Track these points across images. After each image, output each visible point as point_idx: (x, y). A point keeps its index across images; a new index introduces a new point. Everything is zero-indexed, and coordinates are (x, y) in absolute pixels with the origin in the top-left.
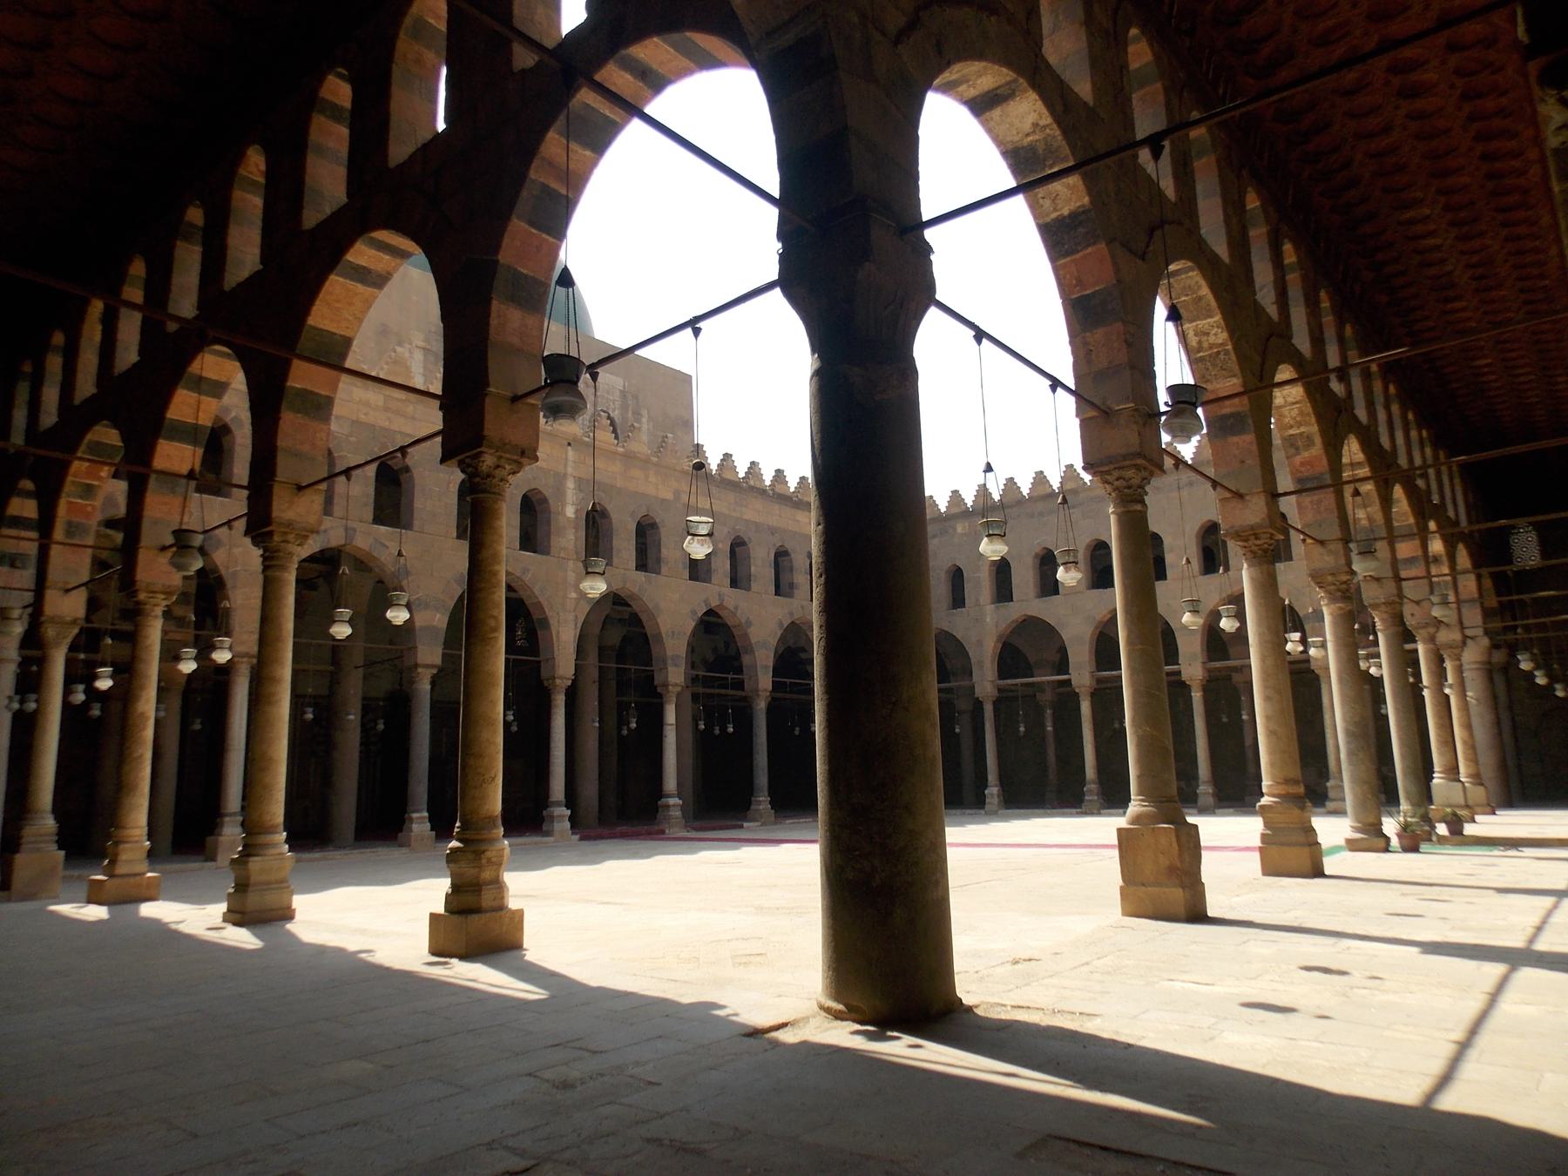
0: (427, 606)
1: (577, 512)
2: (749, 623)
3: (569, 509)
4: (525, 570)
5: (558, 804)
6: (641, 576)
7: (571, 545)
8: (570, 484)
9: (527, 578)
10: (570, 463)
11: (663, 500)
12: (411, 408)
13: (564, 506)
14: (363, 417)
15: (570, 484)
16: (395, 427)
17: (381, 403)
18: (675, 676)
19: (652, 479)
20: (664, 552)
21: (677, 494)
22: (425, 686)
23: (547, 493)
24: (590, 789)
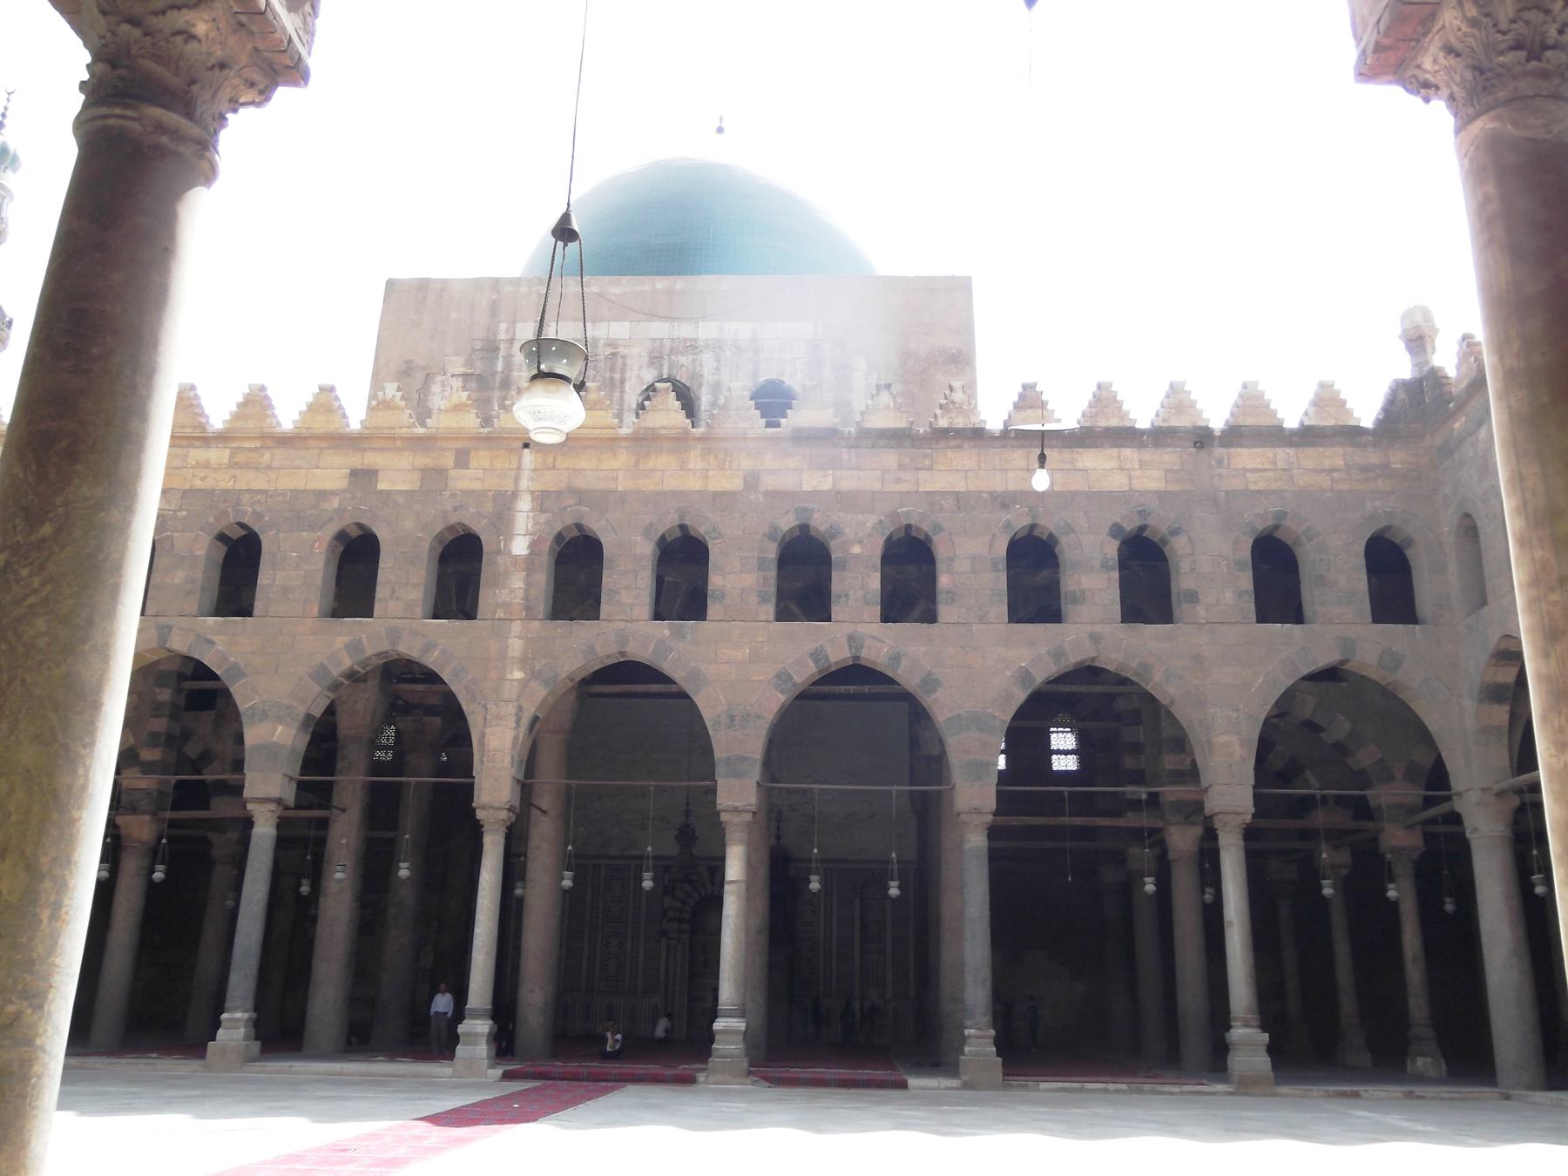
0: (265, 715)
1: (532, 545)
2: (931, 683)
3: (520, 543)
4: (429, 647)
5: (477, 1015)
6: (664, 628)
7: (518, 599)
8: (524, 505)
9: (431, 661)
10: (526, 474)
11: (717, 496)
12: (267, 456)
13: (509, 537)
14: (198, 484)
15: (524, 505)
16: (241, 486)
17: (226, 461)
18: (737, 794)
19: (695, 461)
20: (715, 580)
21: (752, 481)
22: (264, 830)
23: (477, 527)
24: (534, 996)
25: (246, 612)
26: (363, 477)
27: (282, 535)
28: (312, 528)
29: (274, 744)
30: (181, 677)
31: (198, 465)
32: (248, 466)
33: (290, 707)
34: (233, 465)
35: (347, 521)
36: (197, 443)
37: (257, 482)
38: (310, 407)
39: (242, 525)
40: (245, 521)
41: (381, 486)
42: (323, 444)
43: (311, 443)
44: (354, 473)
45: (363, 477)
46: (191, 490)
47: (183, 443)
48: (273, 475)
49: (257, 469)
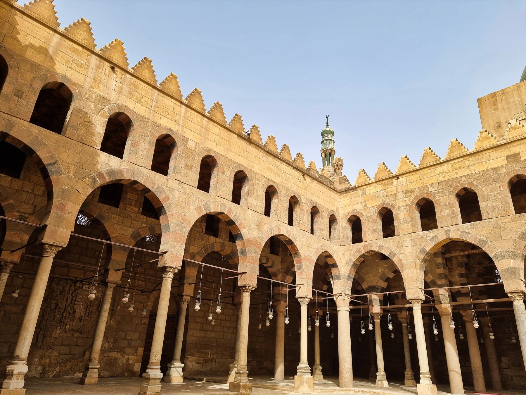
0: (503, 257)
12: (467, 162)
14: (443, 179)
16: (460, 175)
17: (450, 168)
25: (479, 218)
26: (513, 158)
27: (484, 188)
28: (496, 182)
29: (512, 268)
30: (443, 254)
31: (440, 173)
32: (460, 168)
33: (513, 252)
34: (454, 169)
35: (513, 175)
36: (438, 166)
37: (468, 172)
38: (479, 140)
39: (465, 189)
40: (466, 186)
41: (523, 159)
42: (489, 151)
43: (484, 152)
44: (508, 157)
45: (513, 158)
46: (441, 182)
47: (432, 167)
48: (472, 168)
49: (464, 167)
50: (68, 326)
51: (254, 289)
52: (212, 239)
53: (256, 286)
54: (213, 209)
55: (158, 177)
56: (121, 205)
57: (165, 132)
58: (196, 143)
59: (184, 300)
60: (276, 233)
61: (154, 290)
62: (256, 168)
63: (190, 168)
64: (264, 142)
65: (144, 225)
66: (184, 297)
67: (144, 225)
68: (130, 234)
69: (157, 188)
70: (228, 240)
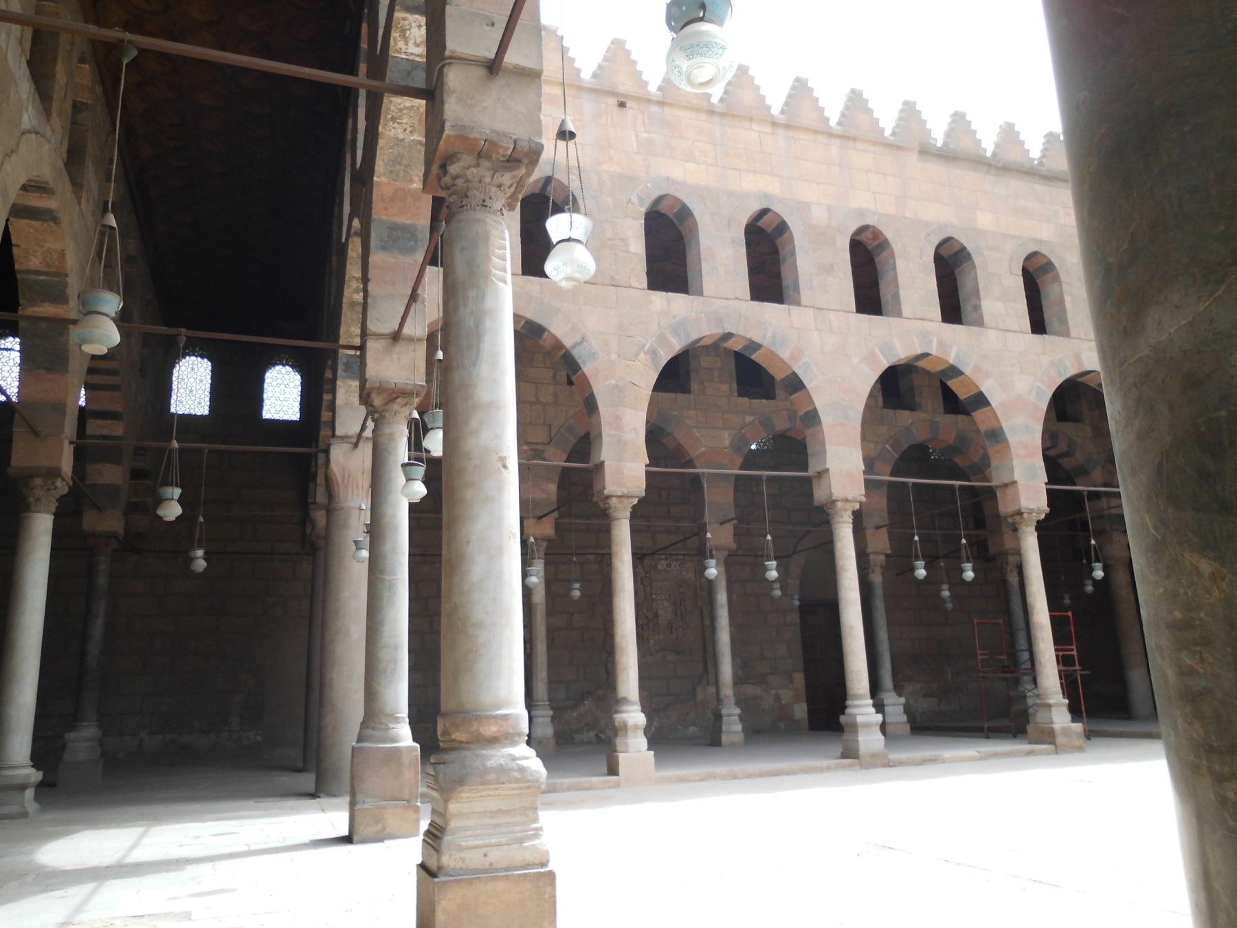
50: (652, 642)
51: (1043, 516)
52: (905, 417)
53: (1048, 510)
54: (902, 352)
55: (770, 311)
56: (694, 386)
57: (756, 207)
58: (829, 208)
59: (872, 563)
60: (1071, 371)
61: (794, 553)
62: (985, 220)
63: (829, 270)
64: (988, 147)
65: (749, 419)
66: (872, 557)
67: (749, 419)
68: (727, 443)
69: (774, 337)
70: (942, 410)
